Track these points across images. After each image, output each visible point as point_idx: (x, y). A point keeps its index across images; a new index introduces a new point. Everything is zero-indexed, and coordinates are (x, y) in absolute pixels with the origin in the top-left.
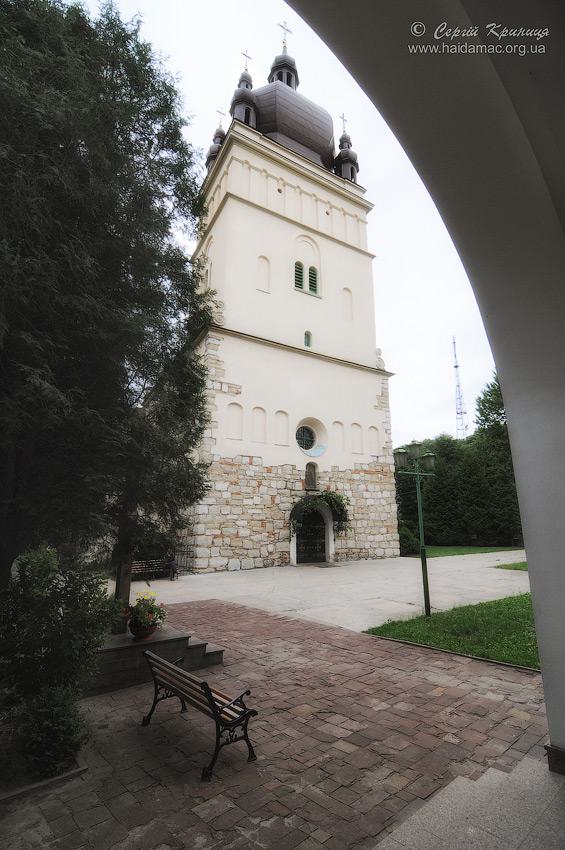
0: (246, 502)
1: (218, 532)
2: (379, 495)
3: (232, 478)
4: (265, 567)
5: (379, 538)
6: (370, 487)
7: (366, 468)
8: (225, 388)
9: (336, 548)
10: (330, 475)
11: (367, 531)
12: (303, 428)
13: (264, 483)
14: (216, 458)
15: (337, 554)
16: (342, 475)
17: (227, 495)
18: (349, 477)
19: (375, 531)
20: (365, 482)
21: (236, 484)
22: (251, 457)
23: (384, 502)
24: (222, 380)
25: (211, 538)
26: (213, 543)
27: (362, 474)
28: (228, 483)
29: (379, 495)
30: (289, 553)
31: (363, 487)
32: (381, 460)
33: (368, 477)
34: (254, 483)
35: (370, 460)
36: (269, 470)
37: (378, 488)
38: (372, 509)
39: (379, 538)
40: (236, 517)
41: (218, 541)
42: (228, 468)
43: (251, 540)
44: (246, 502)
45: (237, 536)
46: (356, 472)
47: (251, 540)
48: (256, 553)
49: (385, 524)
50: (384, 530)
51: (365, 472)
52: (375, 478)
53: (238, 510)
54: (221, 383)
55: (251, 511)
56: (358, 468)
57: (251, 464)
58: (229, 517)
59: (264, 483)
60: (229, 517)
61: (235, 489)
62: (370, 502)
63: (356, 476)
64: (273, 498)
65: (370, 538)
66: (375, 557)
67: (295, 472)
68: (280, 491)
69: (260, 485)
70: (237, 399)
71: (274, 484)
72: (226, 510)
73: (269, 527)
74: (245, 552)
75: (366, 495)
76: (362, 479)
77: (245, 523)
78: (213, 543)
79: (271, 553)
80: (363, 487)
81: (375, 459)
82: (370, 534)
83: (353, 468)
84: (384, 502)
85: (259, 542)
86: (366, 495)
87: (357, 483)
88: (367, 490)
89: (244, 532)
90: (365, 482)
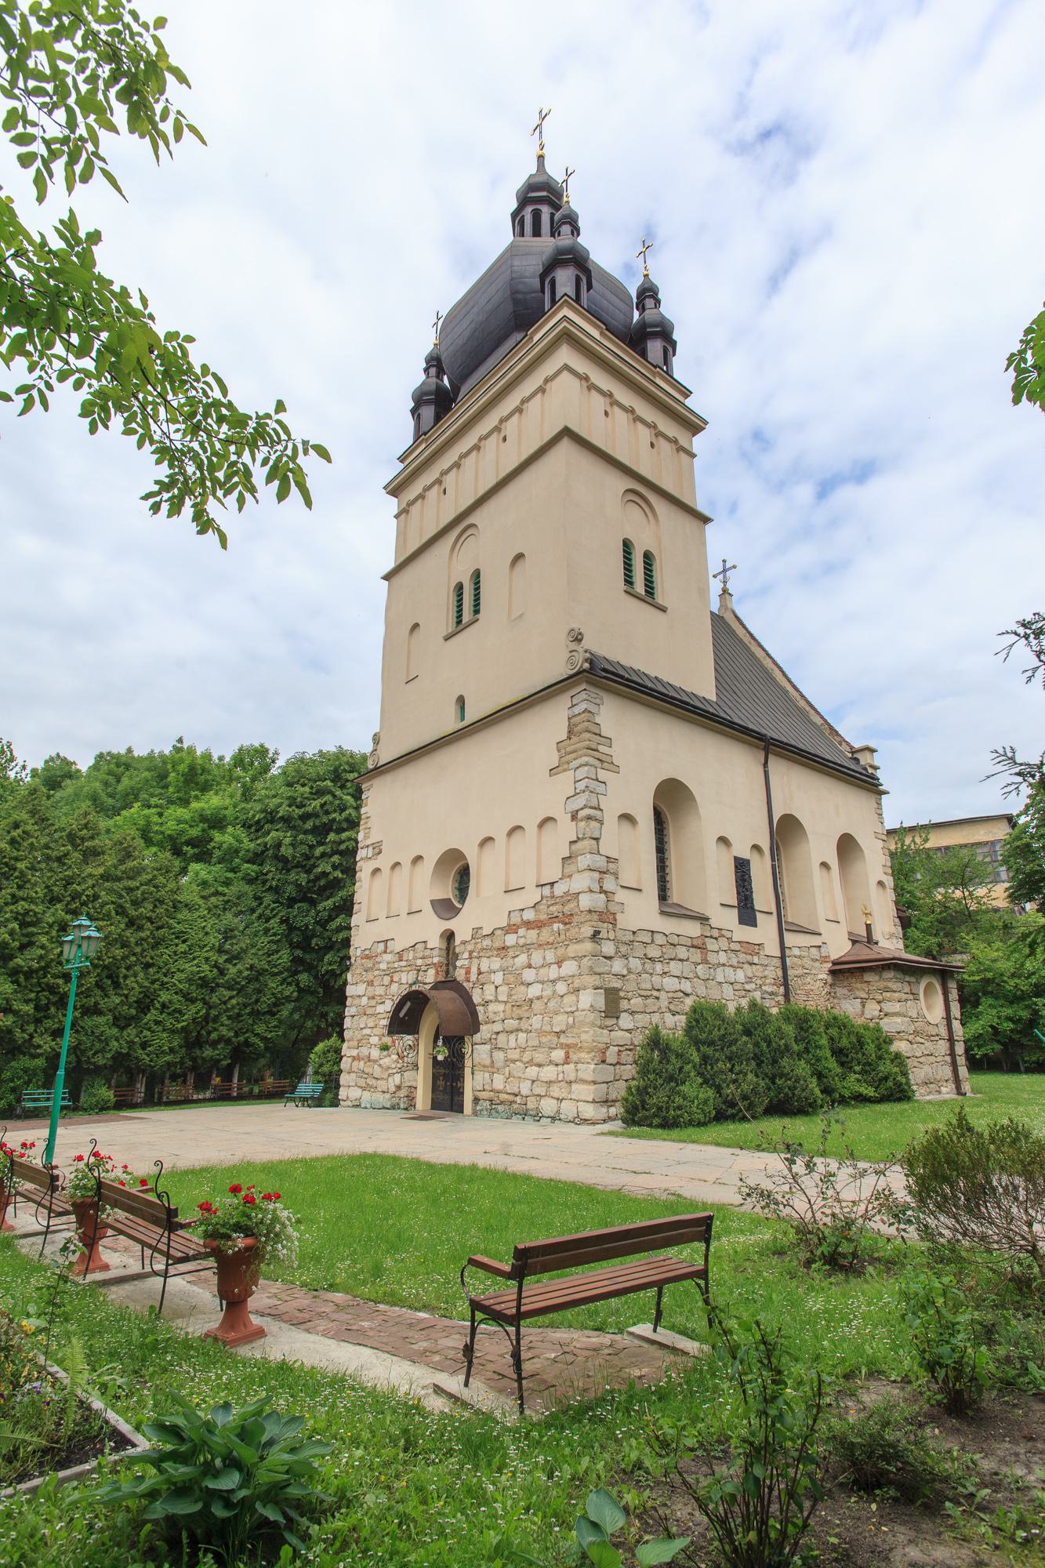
3: (370, 976)
4: (393, 1108)
5: (549, 1073)
6: (537, 957)
7: (529, 915)
10: (470, 947)
11: (526, 1057)
15: (476, 1100)
16: (487, 942)
18: (498, 944)
19: (539, 1057)
20: (527, 948)
29: (553, 972)
31: (522, 959)
32: (559, 890)
33: (532, 935)
34: (387, 980)
35: (534, 896)
36: (400, 955)
37: (550, 956)
38: (538, 1006)
39: (549, 1073)
43: (380, 1065)
46: (511, 929)
49: (563, 1040)
50: (558, 1055)
51: (528, 925)
52: (546, 935)
56: (516, 919)
59: (396, 979)
62: (534, 991)
63: (511, 940)
65: (533, 1071)
66: (538, 1116)
67: (428, 952)
75: (529, 975)
76: (522, 941)
79: (399, 1088)
82: (531, 1063)
86: (529, 975)
87: (511, 954)
88: (530, 966)
90: (527, 948)
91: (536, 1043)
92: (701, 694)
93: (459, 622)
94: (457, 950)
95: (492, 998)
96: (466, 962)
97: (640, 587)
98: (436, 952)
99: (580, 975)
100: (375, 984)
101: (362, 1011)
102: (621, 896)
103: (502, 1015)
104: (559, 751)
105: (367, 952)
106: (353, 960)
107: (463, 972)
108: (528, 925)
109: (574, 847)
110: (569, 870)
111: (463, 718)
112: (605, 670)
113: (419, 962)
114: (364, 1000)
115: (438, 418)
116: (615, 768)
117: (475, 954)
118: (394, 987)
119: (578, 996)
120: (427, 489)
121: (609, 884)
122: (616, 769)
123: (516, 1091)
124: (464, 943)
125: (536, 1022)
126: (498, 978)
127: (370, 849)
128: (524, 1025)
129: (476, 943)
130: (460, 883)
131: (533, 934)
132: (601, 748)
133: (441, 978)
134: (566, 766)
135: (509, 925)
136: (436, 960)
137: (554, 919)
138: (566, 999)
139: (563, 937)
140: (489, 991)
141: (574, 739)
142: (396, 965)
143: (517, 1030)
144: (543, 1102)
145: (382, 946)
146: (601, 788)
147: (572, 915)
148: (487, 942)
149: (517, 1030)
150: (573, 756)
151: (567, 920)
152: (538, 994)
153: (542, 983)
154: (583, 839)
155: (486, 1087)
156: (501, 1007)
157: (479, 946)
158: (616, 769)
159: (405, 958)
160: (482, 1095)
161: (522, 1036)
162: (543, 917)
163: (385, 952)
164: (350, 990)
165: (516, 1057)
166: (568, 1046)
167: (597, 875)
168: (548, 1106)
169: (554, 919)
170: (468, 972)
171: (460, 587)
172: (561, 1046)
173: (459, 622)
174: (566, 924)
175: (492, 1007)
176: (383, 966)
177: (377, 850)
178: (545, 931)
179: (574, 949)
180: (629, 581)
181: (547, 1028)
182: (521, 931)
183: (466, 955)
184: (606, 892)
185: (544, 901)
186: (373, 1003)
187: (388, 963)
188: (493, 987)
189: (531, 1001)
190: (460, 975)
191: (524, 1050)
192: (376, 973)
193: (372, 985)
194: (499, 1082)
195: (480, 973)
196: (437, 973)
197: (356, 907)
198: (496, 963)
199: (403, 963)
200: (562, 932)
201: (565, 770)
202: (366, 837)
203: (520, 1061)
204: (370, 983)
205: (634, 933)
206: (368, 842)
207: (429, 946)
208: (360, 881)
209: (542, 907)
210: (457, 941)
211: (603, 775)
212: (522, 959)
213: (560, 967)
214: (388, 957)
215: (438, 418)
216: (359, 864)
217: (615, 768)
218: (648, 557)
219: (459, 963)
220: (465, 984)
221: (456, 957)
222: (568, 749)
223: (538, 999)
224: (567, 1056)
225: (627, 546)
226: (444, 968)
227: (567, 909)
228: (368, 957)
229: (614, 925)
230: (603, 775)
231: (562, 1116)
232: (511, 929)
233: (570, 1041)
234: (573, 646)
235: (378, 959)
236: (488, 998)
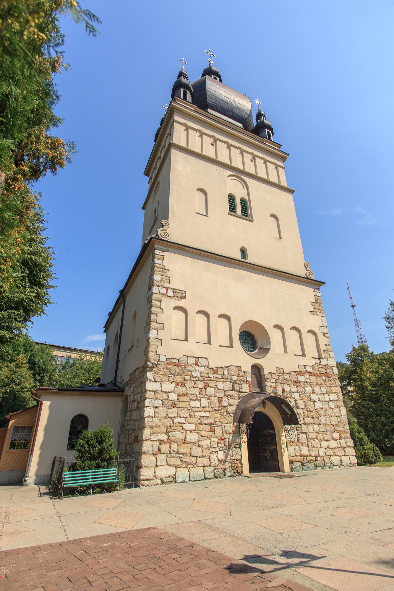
0: (194, 404)
1: (165, 437)
3: (179, 379)
6: (317, 389)
7: (309, 369)
8: (170, 293)
9: (290, 456)
10: (276, 377)
11: (320, 436)
12: (243, 332)
13: (211, 384)
14: (162, 359)
15: (291, 462)
16: (286, 377)
17: (173, 396)
18: (294, 379)
19: (328, 437)
20: (311, 384)
21: (182, 384)
23: (332, 405)
24: (167, 285)
25: (157, 444)
26: (159, 450)
27: (307, 376)
29: (327, 398)
30: (240, 461)
33: (313, 379)
34: (201, 385)
36: (215, 371)
37: (324, 390)
40: (183, 420)
41: (165, 448)
42: (174, 369)
43: (199, 446)
44: (194, 404)
45: (185, 441)
46: (301, 373)
47: (199, 446)
48: (206, 462)
51: (310, 373)
52: (320, 380)
53: (184, 413)
55: (198, 414)
56: (304, 370)
57: (197, 364)
58: (176, 420)
59: (211, 384)
60: (176, 420)
61: (181, 390)
62: (318, 405)
63: (301, 378)
64: (220, 399)
65: (324, 444)
68: (227, 393)
69: (206, 386)
70: (181, 303)
71: (220, 386)
72: (172, 412)
73: (218, 431)
74: (194, 460)
75: (314, 397)
77: (192, 427)
78: (159, 450)
80: (309, 389)
81: (317, 361)
83: (297, 370)
84: (332, 405)
85: (209, 448)
88: (314, 393)
89: (192, 437)
91: (324, 430)
96: (273, 385)
101: (170, 403)
118: (210, 391)
123: (317, 454)
128: (316, 421)
134: (316, 313)
137: (321, 374)
139: (328, 383)
141: (317, 304)
142: (211, 376)
144: (332, 458)
145: (192, 361)
148: (286, 377)
150: (319, 311)
153: (322, 401)
155: (298, 454)
160: (294, 459)
166: (340, 431)
168: (336, 460)
172: (337, 431)
181: (329, 423)
191: (318, 433)
194: (305, 451)
200: (327, 381)
201: (316, 315)
222: (316, 307)
224: (340, 436)
231: (344, 464)
232: (301, 373)
233: (341, 429)
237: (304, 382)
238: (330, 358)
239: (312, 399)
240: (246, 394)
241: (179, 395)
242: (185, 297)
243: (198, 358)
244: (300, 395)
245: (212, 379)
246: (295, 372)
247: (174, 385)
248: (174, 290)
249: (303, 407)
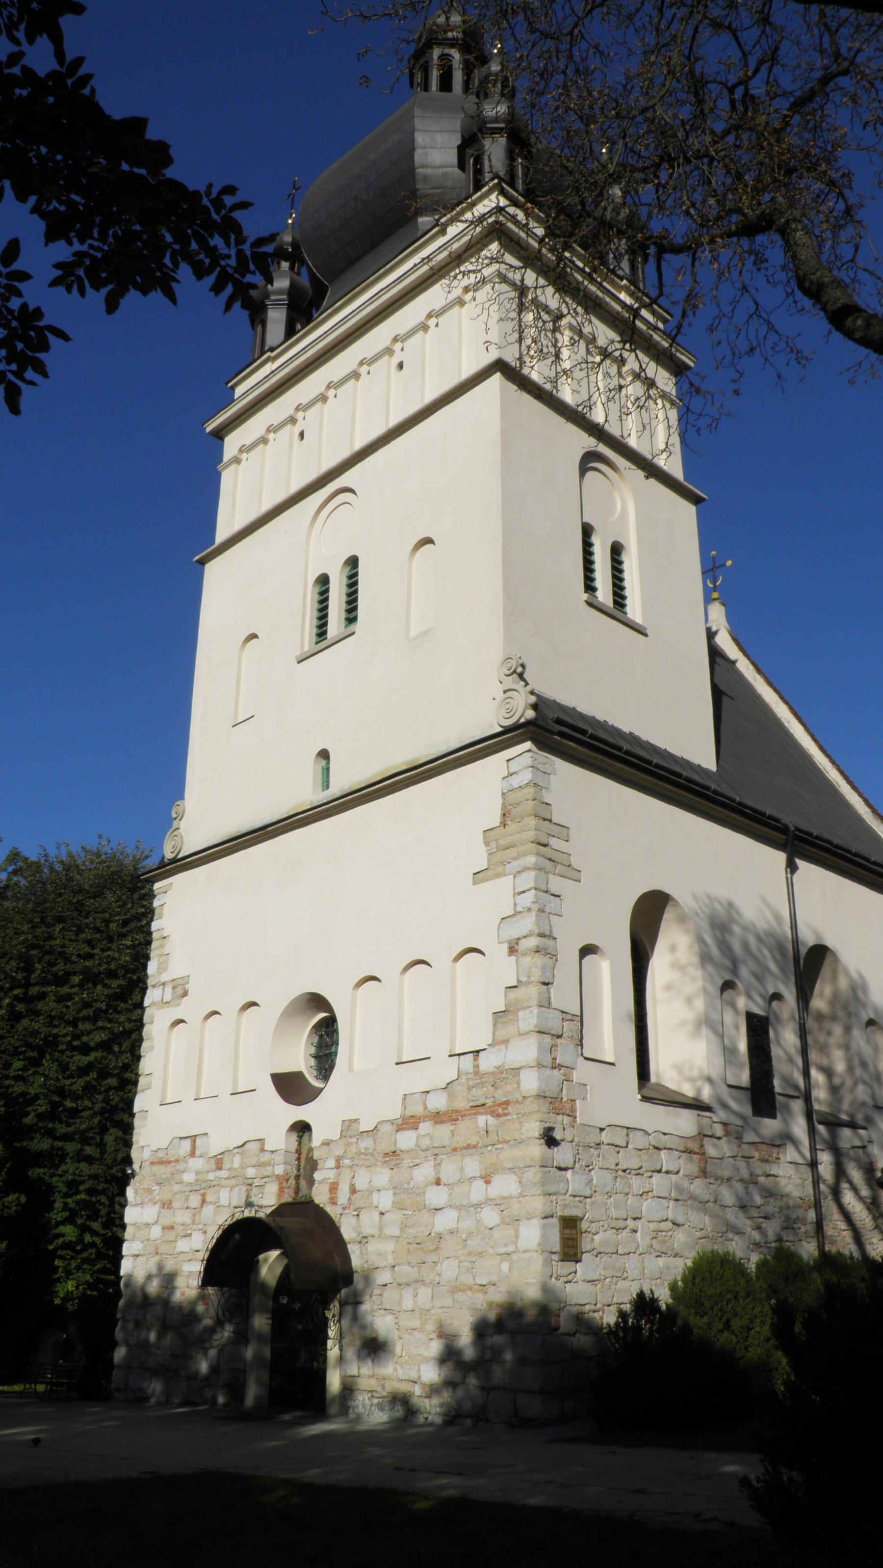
2: (478, 1191)
6: (450, 1169)
7: (438, 1102)
10: (339, 1152)
16: (366, 1143)
18: (386, 1146)
20: (436, 1153)
22: (194, 1138)
23: (490, 1216)
27: (425, 1127)
28: (157, 1207)
29: (478, 1191)
31: (425, 1172)
32: (487, 1062)
34: (195, 1200)
35: (449, 1071)
37: (472, 1166)
38: (449, 1245)
46: (409, 1123)
51: (438, 1118)
54: (164, 984)
56: (416, 1109)
59: (210, 1198)
62: (444, 1221)
63: (406, 1140)
67: (266, 1157)
75: (436, 1196)
76: (425, 1143)
83: (396, 1113)
86: (436, 1196)
87: (407, 1162)
88: (438, 1182)
92: (696, 760)
93: (322, 633)
94: (316, 1155)
95: (374, 1231)
97: (604, 594)
98: (279, 1158)
99: (521, 1195)
100: (175, 1205)
102: (583, 1072)
103: (391, 1260)
104: (487, 844)
105: (161, 1155)
106: (136, 1166)
107: (326, 1189)
108: (438, 1118)
109: (513, 995)
110: (502, 1034)
111: (326, 785)
112: (559, 721)
113: (251, 1172)
114: (156, 1232)
115: (290, 332)
116: (573, 874)
117: (347, 1162)
118: (208, 1211)
119: (517, 1230)
120: (273, 429)
121: (565, 1053)
122: (575, 875)
123: (414, 1375)
124: (326, 1143)
125: (449, 1270)
126: (385, 1200)
127: (169, 989)
129: (348, 1145)
130: (320, 1046)
131: (445, 1130)
132: (554, 842)
133: (288, 1198)
134: (500, 869)
135: (404, 1118)
136: (279, 1170)
137: (479, 1108)
138: (497, 1234)
139: (493, 1137)
140: (369, 1222)
141: (512, 826)
142: (211, 1176)
143: (417, 1281)
145: (186, 1145)
146: (552, 905)
147: (507, 1103)
148: (366, 1143)
149: (417, 1281)
150: (513, 852)
151: (500, 1109)
152: (452, 1225)
153: (459, 1208)
154: (528, 983)
156: (390, 1247)
157: (353, 1149)
158: (575, 875)
159: (226, 1165)
161: (424, 1293)
162: (461, 1104)
163: (193, 1154)
164: (130, 1215)
165: (416, 1323)
167: (547, 1039)
169: (479, 1108)
170: (334, 1188)
171: (324, 580)
173: (322, 633)
174: (498, 1116)
175: (373, 1247)
176: (189, 1177)
177: (180, 991)
178: (464, 1125)
179: (509, 1154)
180: (590, 587)
181: (467, 1279)
182: (425, 1127)
183: (331, 1163)
184: (560, 1066)
185: (463, 1080)
186: (171, 1236)
187: (197, 1173)
188: (376, 1216)
189: (440, 1236)
190: (320, 1196)
192: (177, 1188)
193: (169, 1208)
195: (353, 1191)
196: (281, 1190)
197: (142, 1081)
198: (383, 1176)
199: (223, 1174)
201: (498, 875)
202: (162, 969)
203: (422, 1330)
204: (167, 1205)
205: (602, 1130)
206: (165, 977)
207: (268, 1147)
208: (151, 1039)
209: (458, 1088)
210: (317, 1138)
211: (556, 884)
212: (425, 1172)
213: (488, 1182)
214: (196, 1164)
215: (290, 332)
216: (147, 1013)
217: (573, 874)
218: (616, 550)
219: (317, 1176)
220: (329, 1209)
221: (313, 1165)
222: (502, 842)
223: (452, 1232)
225: (587, 531)
226: (292, 1181)
227: (500, 1096)
228: (161, 1162)
229: (572, 1115)
230: (556, 884)
232: (409, 1123)
234: (510, 682)
235: (181, 1166)
236: (367, 1231)
237: (412, 1150)
238: (520, 1035)
239: (427, 1203)
240: (273, 1208)
241: (164, 1228)
242: (185, 994)
243: (196, 1136)
244: (395, 1194)
245: (213, 1184)
246: (392, 1122)
247: (157, 1207)
248: (175, 983)
249: (397, 1233)
